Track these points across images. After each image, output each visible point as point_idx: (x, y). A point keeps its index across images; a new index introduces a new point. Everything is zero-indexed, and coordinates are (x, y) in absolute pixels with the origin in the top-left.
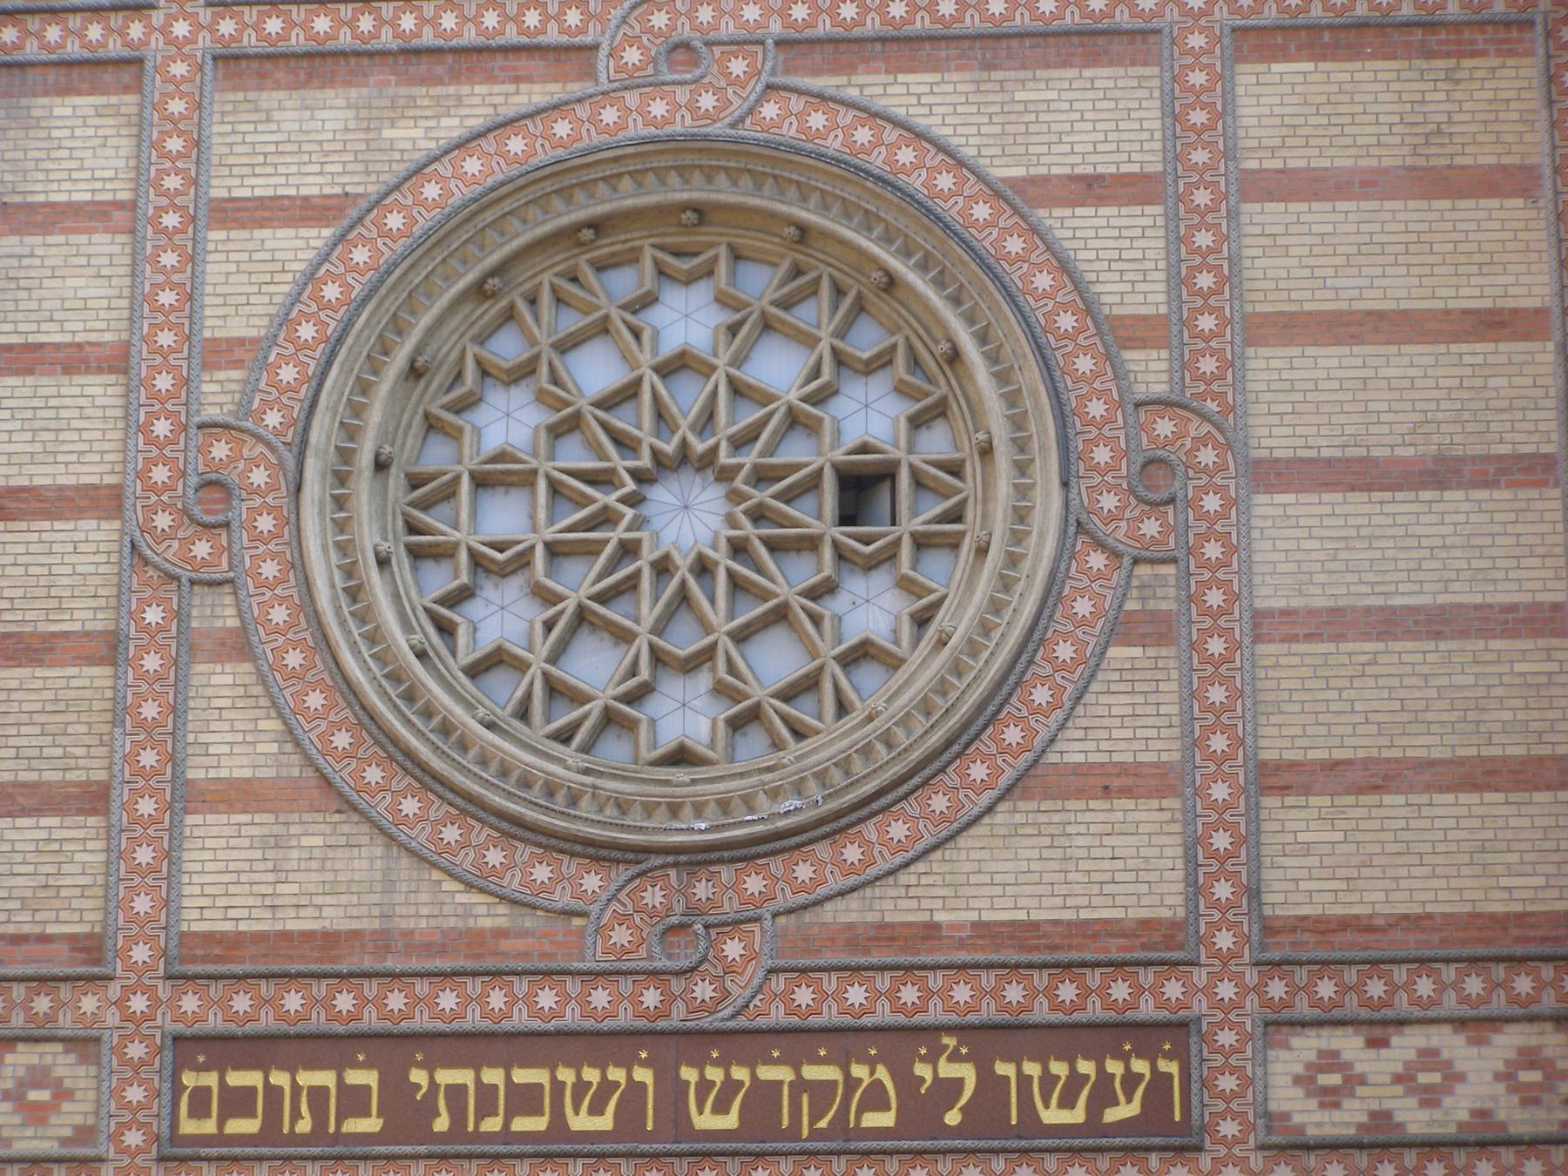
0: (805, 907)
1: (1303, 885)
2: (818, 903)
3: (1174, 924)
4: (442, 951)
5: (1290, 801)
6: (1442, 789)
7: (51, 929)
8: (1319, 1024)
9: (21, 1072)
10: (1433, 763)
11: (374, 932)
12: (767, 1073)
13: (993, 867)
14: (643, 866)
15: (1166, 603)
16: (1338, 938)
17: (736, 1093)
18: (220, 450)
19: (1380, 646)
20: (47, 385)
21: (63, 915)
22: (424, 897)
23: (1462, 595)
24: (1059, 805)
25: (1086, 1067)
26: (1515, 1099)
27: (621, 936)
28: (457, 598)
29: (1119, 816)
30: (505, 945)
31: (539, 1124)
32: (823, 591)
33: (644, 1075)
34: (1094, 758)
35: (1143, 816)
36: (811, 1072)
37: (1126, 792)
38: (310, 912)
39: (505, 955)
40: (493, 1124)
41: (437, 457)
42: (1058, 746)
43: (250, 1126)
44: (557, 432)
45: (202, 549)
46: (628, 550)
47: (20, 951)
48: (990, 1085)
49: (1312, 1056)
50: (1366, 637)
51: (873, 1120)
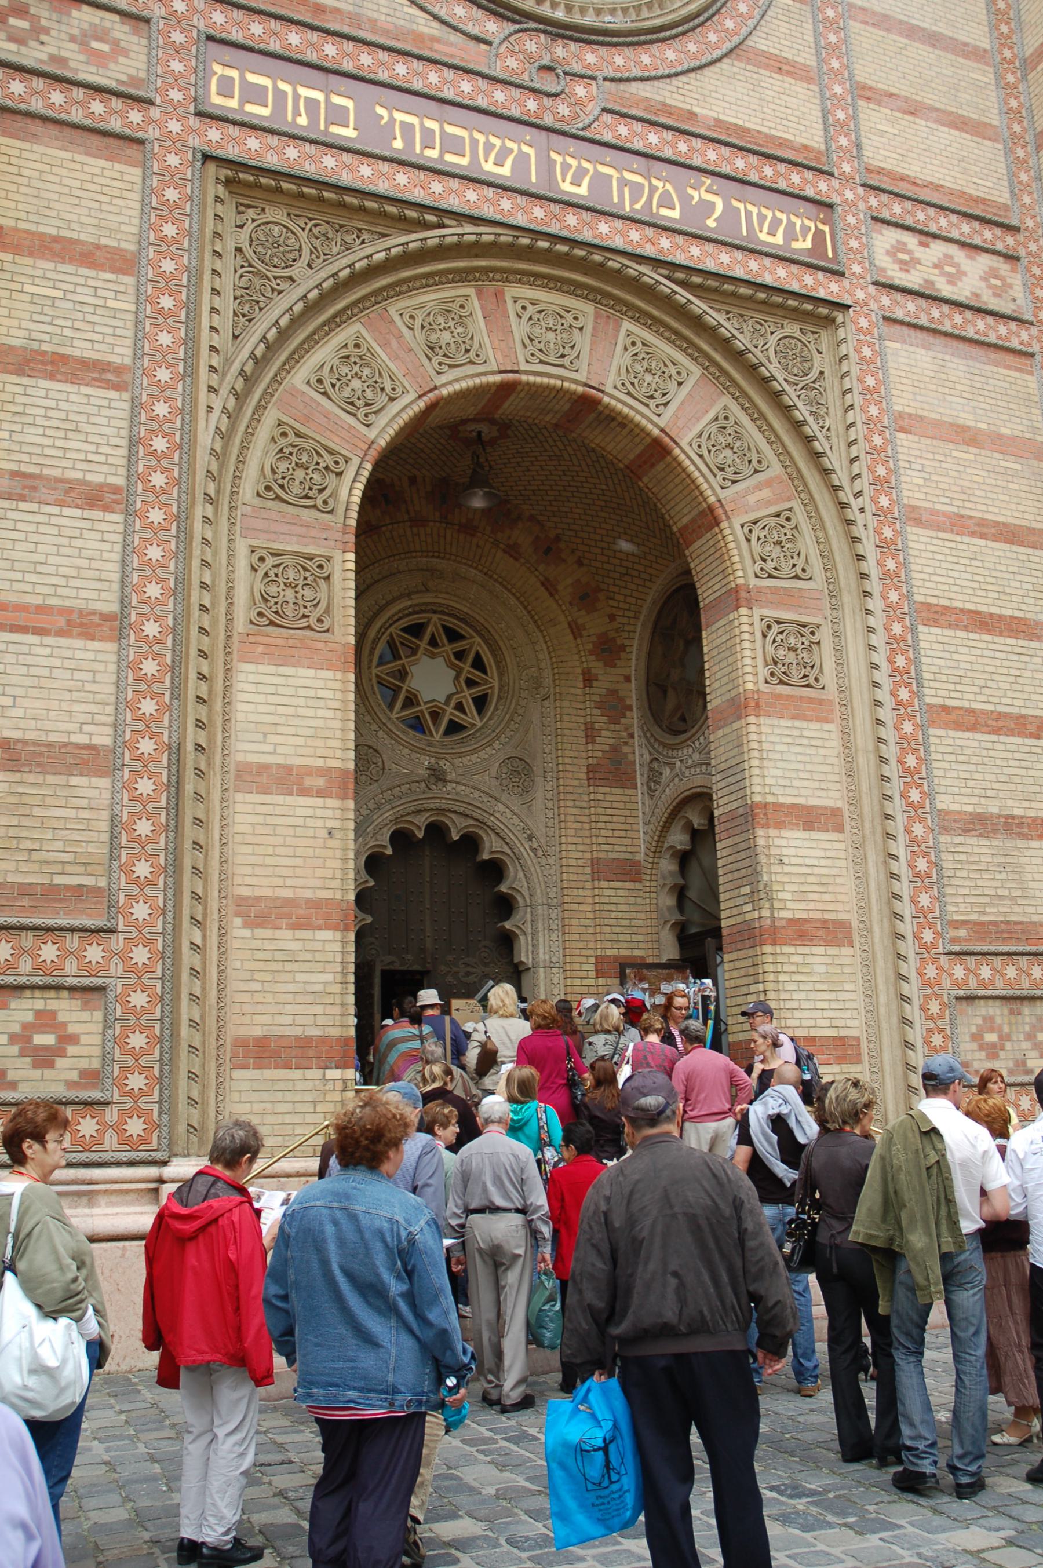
0: (621, 80)
2: (628, 80)
3: (819, 152)
5: (871, 106)
6: (944, 125)
8: (896, 225)
10: (937, 110)
12: (603, 169)
13: (723, 91)
14: (525, 26)
16: (901, 184)
17: (585, 175)
24: (756, 69)
26: (990, 292)
27: (512, 63)
29: (787, 86)
30: (436, 46)
31: (464, 161)
34: (772, 50)
35: (800, 90)
36: (628, 176)
37: (789, 73)
42: (752, 38)
43: (265, 112)
49: (894, 242)
50: (901, 34)
51: (664, 212)
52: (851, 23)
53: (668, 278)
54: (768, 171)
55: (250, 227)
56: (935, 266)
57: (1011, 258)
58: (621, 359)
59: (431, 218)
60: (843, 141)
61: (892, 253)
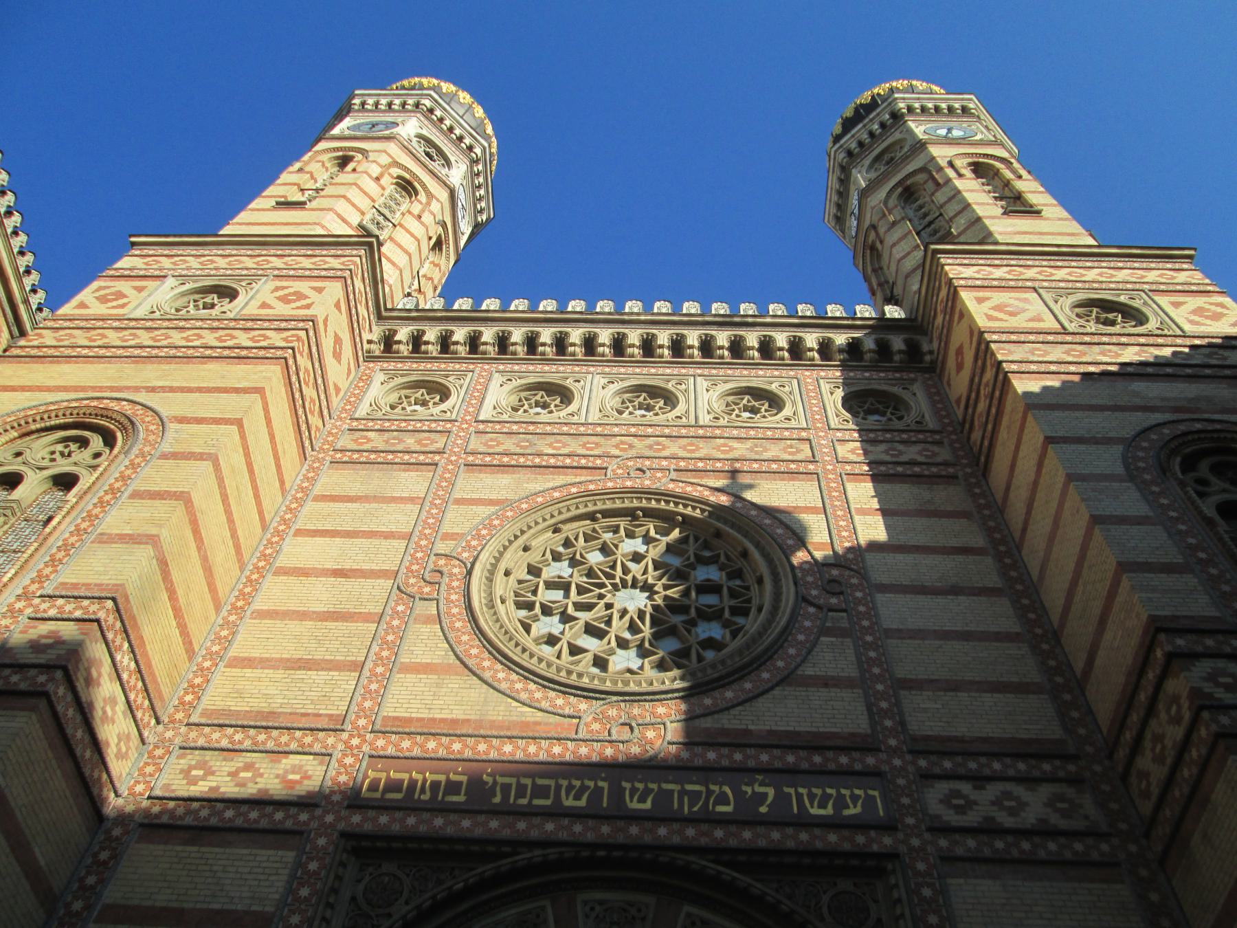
1: (927, 723)
4: (508, 729)
5: (913, 692)
7: (321, 712)
9: (289, 767)
11: (476, 720)
12: (665, 786)
17: (648, 795)
18: (442, 562)
19: (942, 642)
20: (376, 542)
21: (329, 707)
22: (502, 708)
23: (972, 627)
25: (829, 791)
31: (548, 802)
32: (692, 623)
33: (601, 784)
34: (818, 673)
36: (689, 787)
37: (835, 686)
38: (447, 711)
39: (538, 731)
40: (524, 801)
47: (304, 719)
48: (781, 798)
52: (889, 641)
53: (713, 861)
54: (817, 759)
55: (367, 878)
56: (993, 803)
57: (1075, 781)
59: (507, 849)
60: (888, 723)
61: (946, 801)
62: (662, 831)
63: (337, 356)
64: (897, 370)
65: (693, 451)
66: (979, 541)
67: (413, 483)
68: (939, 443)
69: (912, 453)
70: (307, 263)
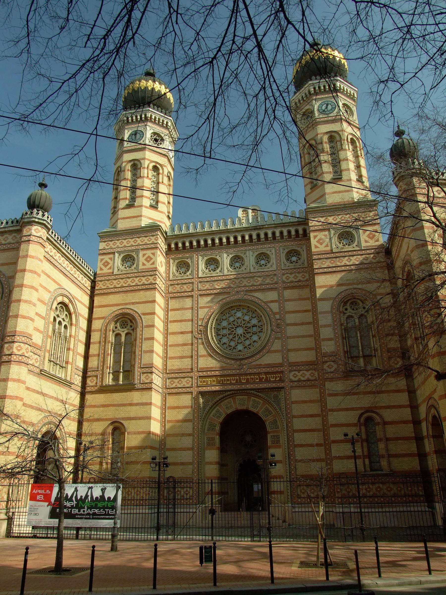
15: (280, 336)
28: (221, 339)
41: (219, 327)
44: (229, 324)
45: (200, 335)
46: (235, 334)
48: (267, 377)
57: (315, 370)
58: (251, 402)
62: (248, 386)
63: (162, 266)
64: (300, 240)
65: (249, 283)
66: (310, 308)
67: (188, 303)
68: (306, 272)
69: (300, 277)
70: (146, 240)
